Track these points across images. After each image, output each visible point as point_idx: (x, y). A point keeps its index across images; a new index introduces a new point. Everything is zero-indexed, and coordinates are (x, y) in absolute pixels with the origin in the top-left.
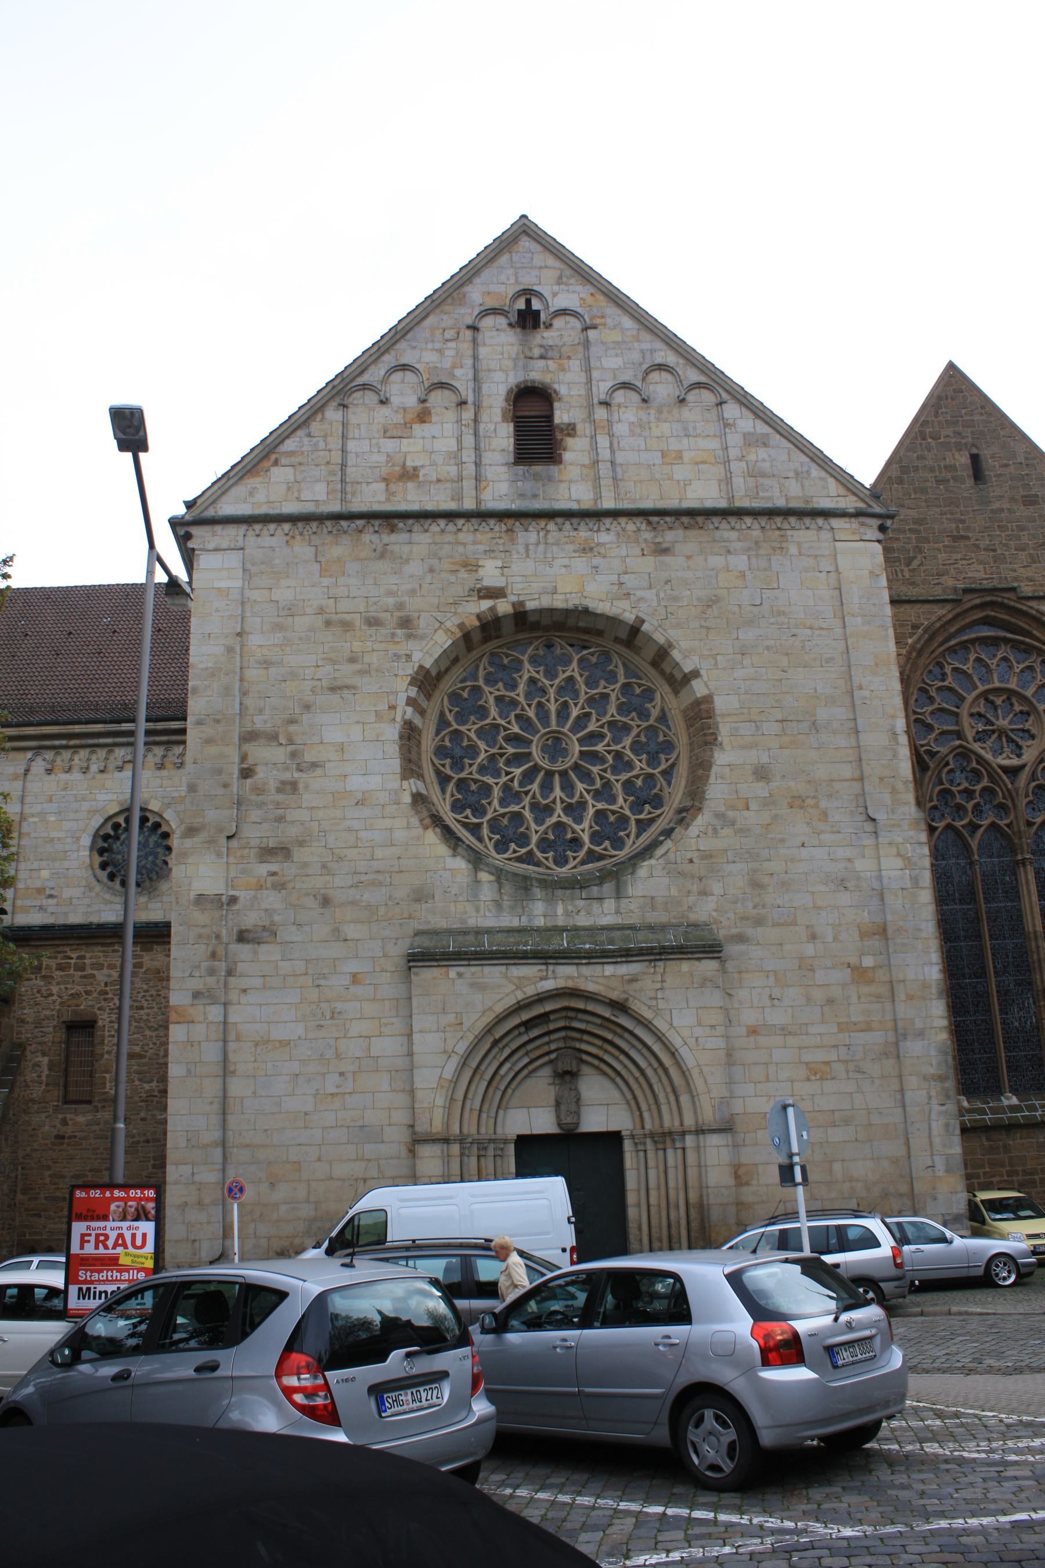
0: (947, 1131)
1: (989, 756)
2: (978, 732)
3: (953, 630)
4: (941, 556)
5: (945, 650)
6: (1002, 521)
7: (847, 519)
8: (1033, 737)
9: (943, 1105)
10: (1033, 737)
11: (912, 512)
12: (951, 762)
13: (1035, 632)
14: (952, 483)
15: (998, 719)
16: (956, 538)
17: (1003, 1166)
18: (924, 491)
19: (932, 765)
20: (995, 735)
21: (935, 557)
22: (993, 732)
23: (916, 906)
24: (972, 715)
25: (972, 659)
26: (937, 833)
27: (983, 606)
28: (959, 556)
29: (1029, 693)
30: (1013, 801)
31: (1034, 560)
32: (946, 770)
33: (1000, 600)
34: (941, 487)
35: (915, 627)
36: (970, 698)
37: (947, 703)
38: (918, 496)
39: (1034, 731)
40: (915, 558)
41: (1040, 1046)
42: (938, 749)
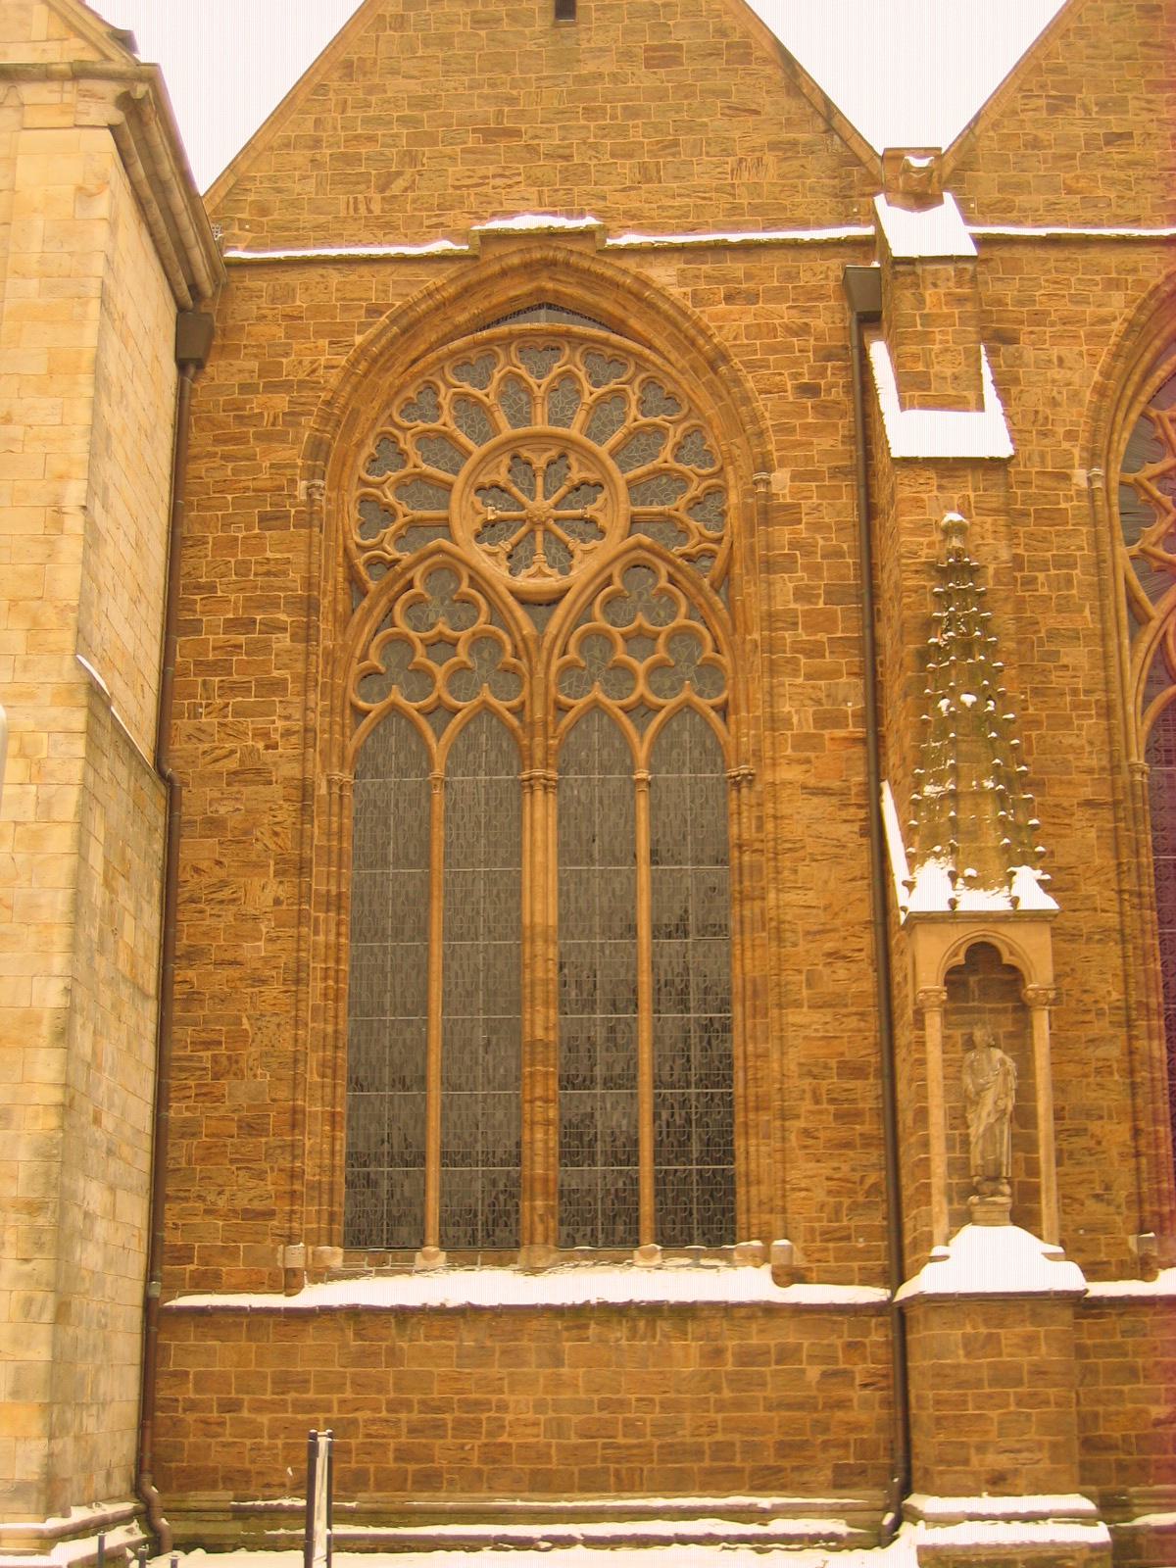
0: (27, 1314)
1: (496, 570)
2: (489, 525)
3: (461, 318)
4: (454, 171)
5: (439, 359)
6: (594, 99)
7: (55, 86)
8: (602, 533)
9: (27, 1260)
10: (602, 533)
11: (412, 85)
12: (417, 583)
13: (633, 322)
14: (505, 25)
15: (533, 499)
16: (490, 135)
17: (380, 1391)
18: (445, 41)
19: (372, 585)
20: (524, 529)
21: (442, 173)
22: (522, 521)
23: (40, 857)
24: (480, 489)
25: (497, 376)
26: (366, 721)
27: (530, 269)
28: (492, 170)
29: (603, 451)
30: (530, 660)
31: (646, 175)
32: (404, 597)
33: (561, 256)
34: (483, 33)
35: (374, 311)
36: (478, 451)
37: (436, 464)
38: (430, 51)
39: (602, 522)
40: (399, 174)
41: (519, 1156)
42: (397, 555)
